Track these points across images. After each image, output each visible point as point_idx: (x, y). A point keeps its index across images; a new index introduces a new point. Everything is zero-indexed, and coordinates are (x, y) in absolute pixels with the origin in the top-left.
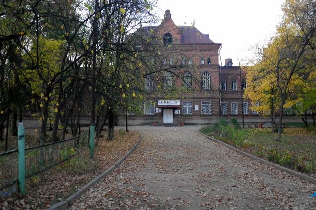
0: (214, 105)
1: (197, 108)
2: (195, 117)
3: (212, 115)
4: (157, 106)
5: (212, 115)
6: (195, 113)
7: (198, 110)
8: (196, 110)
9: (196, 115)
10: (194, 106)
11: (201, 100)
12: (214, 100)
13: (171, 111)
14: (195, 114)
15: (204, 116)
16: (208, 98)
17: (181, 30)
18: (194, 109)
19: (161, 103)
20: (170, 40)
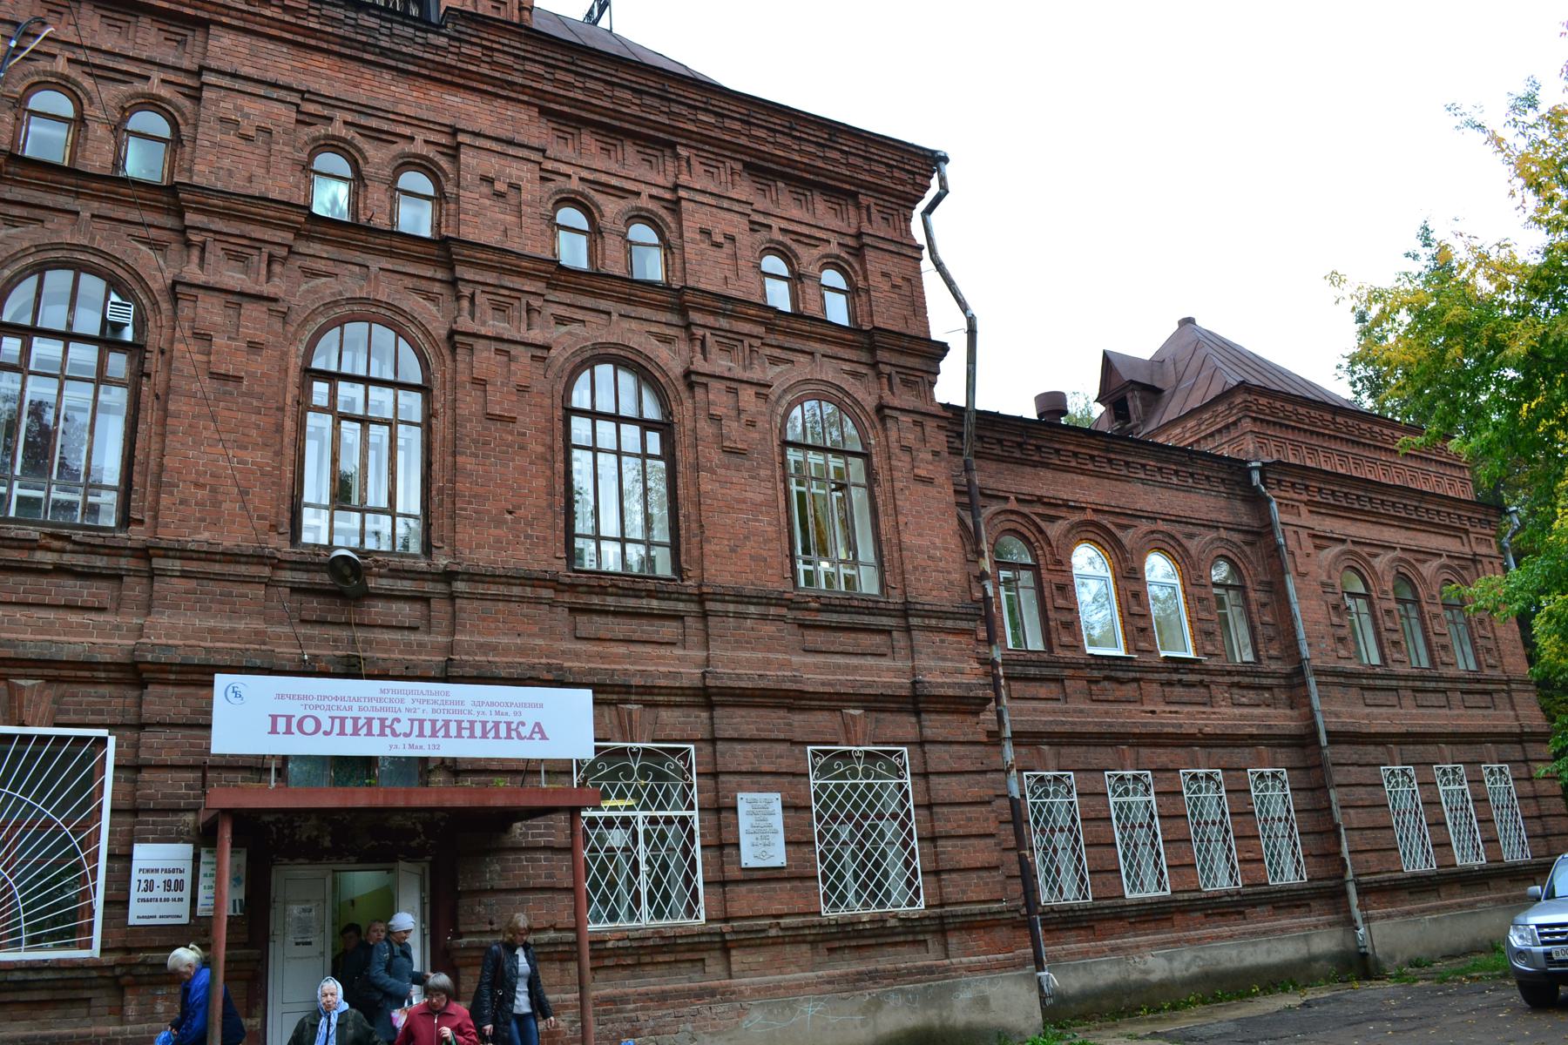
1: (761, 831)
3: (939, 926)
5: (939, 926)
6: (744, 901)
7: (777, 856)
8: (750, 856)
9: (755, 940)
10: (721, 811)
11: (800, 722)
12: (936, 726)
16: (876, 703)
18: (724, 845)
19: (252, 716)
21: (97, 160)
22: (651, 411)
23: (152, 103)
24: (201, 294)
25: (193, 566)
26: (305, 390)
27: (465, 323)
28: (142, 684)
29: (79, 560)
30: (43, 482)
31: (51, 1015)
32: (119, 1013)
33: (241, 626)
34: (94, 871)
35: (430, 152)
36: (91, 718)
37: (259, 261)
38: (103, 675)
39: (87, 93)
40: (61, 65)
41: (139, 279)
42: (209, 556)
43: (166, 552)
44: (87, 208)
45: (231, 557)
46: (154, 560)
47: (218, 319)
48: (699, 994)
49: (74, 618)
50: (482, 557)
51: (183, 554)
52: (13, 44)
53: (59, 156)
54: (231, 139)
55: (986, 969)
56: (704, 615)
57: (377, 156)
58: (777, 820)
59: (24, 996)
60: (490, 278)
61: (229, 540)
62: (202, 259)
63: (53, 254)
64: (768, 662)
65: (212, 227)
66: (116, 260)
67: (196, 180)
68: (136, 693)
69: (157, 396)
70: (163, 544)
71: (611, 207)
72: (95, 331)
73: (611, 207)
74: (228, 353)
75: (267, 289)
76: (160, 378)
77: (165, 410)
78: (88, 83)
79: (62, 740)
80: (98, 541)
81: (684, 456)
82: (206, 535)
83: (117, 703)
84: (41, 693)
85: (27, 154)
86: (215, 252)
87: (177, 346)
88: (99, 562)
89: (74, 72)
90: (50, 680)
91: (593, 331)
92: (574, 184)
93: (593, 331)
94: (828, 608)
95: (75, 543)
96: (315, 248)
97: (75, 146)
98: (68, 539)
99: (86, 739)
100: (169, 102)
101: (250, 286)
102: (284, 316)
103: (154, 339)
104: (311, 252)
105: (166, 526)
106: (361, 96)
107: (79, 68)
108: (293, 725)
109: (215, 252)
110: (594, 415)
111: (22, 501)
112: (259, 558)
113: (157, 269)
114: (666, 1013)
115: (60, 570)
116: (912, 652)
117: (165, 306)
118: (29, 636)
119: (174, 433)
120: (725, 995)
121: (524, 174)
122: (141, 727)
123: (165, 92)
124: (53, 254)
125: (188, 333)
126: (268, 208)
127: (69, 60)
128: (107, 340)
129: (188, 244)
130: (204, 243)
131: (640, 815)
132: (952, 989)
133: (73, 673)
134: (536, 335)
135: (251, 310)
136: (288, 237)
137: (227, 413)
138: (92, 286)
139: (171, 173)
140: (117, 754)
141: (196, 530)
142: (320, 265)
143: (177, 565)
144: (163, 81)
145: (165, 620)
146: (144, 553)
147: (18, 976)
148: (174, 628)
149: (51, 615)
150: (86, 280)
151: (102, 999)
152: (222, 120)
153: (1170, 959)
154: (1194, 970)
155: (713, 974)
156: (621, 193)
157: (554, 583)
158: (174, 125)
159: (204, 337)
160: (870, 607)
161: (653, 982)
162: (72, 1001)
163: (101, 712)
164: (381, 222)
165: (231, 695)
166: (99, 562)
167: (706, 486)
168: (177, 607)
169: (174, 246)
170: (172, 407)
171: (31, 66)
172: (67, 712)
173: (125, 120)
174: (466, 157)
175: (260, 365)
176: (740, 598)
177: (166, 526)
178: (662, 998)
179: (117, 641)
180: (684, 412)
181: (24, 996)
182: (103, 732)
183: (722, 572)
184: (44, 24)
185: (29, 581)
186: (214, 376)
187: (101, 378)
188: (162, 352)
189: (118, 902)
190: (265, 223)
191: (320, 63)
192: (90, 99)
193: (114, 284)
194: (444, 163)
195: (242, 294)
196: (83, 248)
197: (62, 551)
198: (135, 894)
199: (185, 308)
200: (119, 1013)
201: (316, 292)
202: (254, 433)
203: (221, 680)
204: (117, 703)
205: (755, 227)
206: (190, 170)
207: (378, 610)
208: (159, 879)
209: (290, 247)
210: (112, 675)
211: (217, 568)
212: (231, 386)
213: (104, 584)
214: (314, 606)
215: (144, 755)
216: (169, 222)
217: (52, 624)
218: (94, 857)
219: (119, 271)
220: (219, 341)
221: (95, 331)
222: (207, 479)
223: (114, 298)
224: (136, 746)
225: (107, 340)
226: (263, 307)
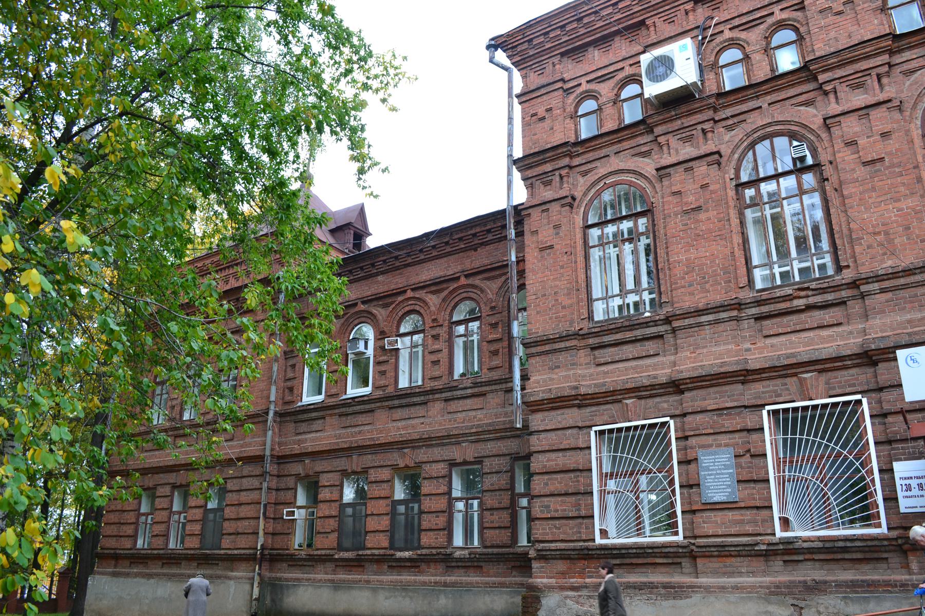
21: (762, 73)
23: (781, 25)
24: (841, 118)
25: (886, 284)
28: (875, 364)
29: (818, 299)
30: (787, 261)
31: (866, 567)
32: (906, 566)
34: (873, 481)
36: (849, 390)
37: (872, 82)
38: (849, 363)
39: (744, 41)
40: (728, 34)
41: (805, 126)
42: (894, 275)
43: (867, 280)
44: (764, 102)
45: (908, 272)
46: (861, 287)
47: (857, 129)
49: (824, 333)
51: (878, 278)
52: (700, 38)
53: (743, 82)
54: (831, 19)
59: (847, 556)
62: (837, 98)
63: (755, 135)
65: (836, 76)
66: (788, 122)
67: (818, 54)
68: (873, 370)
69: (836, 190)
70: (863, 276)
72: (789, 166)
74: (871, 147)
75: (882, 97)
76: (834, 179)
77: (843, 196)
78: (743, 35)
79: (835, 405)
80: (826, 285)
82: (889, 263)
83: (862, 378)
84: (817, 380)
85: (728, 88)
86: (843, 89)
87: (837, 155)
88: (830, 297)
89: (735, 34)
90: (820, 371)
95: (813, 290)
96: (907, 55)
97: (748, 72)
98: (808, 289)
99: (849, 402)
100: (789, 19)
101: (873, 100)
102: (900, 108)
103: (824, 157)
104: (905, 59)
105: (863, 264)
107: (737, 30)
109: (843, 89)
111: (800, 270)
113: (812, 116)
115: (809, 308)
117: (824, 135)
118: (802, 349)
119: (851, 207)
122: (881, 389)
123: (784, 15)
124: (755, 135)
125: (843, 145)
126: (865, 47)
127: (730, 29)
128: (799, 168)
129: (826, 93)
130: (835, 88)
133: (832, 365)
135: (875, 114)
136: (885, 58)
137: (881, 183)
138: (781, 142)
139: (804, 58)
140: (870, 409)
141: (883, 261)
142: (914, 64)
143: (876, 286)
144: (781, 10)
145: (878, 321)
146: (854, 285)
147: (841, 544)
148: (880, 327)
149: (811, 334)
150: (776, 140)
151: (895, 559)
152: (821, 12)
158: (796, 30)
159: (851, 143)
162: (878, 559)
163: (854, 385)
165: (910, 362)
166: (830, 297)
168: (883, 312)
169: (818, 99)
170: (845, 193)
171: (713, 44)
172: (834, 388)
173: (769, 43)
175: (893, 144)
177: (863, 264)
179: (852, 341)
181: (847, 556)
182: (858, 397)
184: (712, 18)
185: (794, 318)
186: (865, 164)
187: (802, 192)
188: (831, 163)
189: (891, 499)
190: (868, 57)
192: (748, 43)
193: (792, 136)
195: (867, 107)
196: (770, 124)
197: (807, 296)
198: (900, 494)
199: (835, 131)
200: (906, 566)
201: (917, 83)
202: (902, 189)
203: (900, 354)
204: (862, 378)
206: (813, 51)
208: (914, 483)
209: (889, 63)
210: (855, 362)
211: (902, 281)
212: (878, 166)
213: (836, 309)
215: (886, 407)
216: (811, 86)
217: (813, 339)
218: (871, 472)
219: (793, 128)
220: (862, 142)
221: (789, 166)
222: (881, 228)
223: (795, 143)
224: (880, 402)
225: (799, 168)
226: (883, 108)
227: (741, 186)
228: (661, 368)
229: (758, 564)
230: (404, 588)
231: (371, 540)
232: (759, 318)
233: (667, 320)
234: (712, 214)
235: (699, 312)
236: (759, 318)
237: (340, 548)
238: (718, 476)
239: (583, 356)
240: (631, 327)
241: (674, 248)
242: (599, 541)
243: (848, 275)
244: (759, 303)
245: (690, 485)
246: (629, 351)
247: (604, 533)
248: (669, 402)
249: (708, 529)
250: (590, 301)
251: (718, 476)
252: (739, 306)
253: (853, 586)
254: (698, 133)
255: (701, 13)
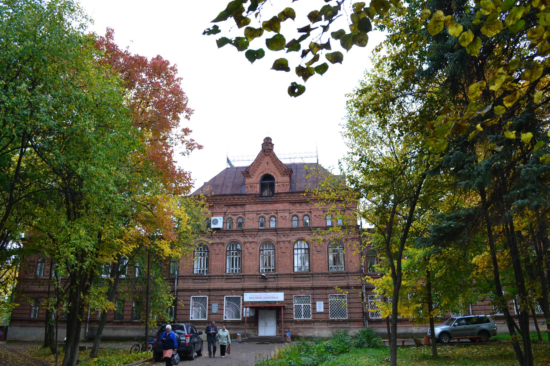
0: (352, 300)
1: (320, 307)
2: (317, 325)
3: (349, 321)
4: (245, 304)
5: (349, 321)
6: (317, 316)
7: (322, 310)
8: (318, 310)
9: (318, 321)
10: (314, 304)
11: (328, 291)
13: (273, 313)
14: (319, 320)
15: (333, 322)
17: (289, 171)
18: (314, 308)
19: (248, 297)
20: (272, 186)
22: (307, 247)
26: (260, 252)
27: (280, 240)
33: (254, 283)
35: (274, 214)
37: (253, 236)
40: (230, 216)
42: (249, 275)
44: (234, 234)
48: (309, 328)
50: (281, 272)
51: (247, 276)
55: (357, 328)
56: (313, 277)
57: (267, 217)
58: (322, 305)
60: (282, 232)
61: (252, 273)
64: (322, 283)
71: (300, 215)
73: (300, 215)
74: (250, 250)
81: (311, 253)
91: (298, 236)
92: (295, 213)
93: (298, 236)
94: (333, 274)
96: (260, 233)
103: (243, 249)
106: (265, 209)
108: (251, 298)
109: (248, 236)
110: (298, 249)
112: (255, 275)
114: (304, 330)
116: (348, 279)
120: (313, 328)
121: (287, 214)
131: (302, 305)
132: (349, 330)
134: (289, 239)
135: (253, 244)
146: (243, 276)
151: (242, 324)
153: (419, 329)
154: (425, 331)
155: (312, 325)
156: (302, 212)
157: (291, 274)
160: (341, 273)
161: (304, 326)
164: (268, 227)
167: (314, 257)
174: (279, 214)
175: (254, 250)
176: (318, 274)
178: (304, 328)
180: (311, 246)
183: (315, 270)
189: (243, 314)
191: (259, 205)
194: (276, 215)
205: (324, 212)
207: (269, 280)
214: (262, 280)
227: (227, 251)
228: (206, 286)
229: (220, 324)
230: (136, 329)
231: (125, 317)
232: (226, 279)
233: (209, 276)
234: (221, 256)
235: (215, 276)
236: (226, 279)
237: (115, 319)
238: (215, 309)
239: (190, 281)
240: (202, 276)
241: (212, 261)
242: (190, 319)
243: (242, 274)
244: (227, 276)
245: (210, 309)
246: (200, 281)
247: (192, 318)
248: (207, 293)
249: (212, 318)
250: (193, 269)
251: (215, 310)
252: (223, 276)
253: (235, 328)
254: (220, 237)
255: (225, 209)
